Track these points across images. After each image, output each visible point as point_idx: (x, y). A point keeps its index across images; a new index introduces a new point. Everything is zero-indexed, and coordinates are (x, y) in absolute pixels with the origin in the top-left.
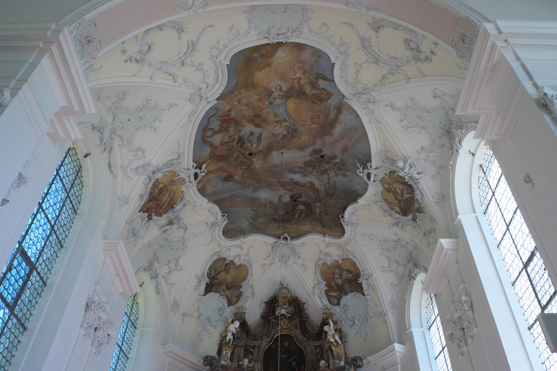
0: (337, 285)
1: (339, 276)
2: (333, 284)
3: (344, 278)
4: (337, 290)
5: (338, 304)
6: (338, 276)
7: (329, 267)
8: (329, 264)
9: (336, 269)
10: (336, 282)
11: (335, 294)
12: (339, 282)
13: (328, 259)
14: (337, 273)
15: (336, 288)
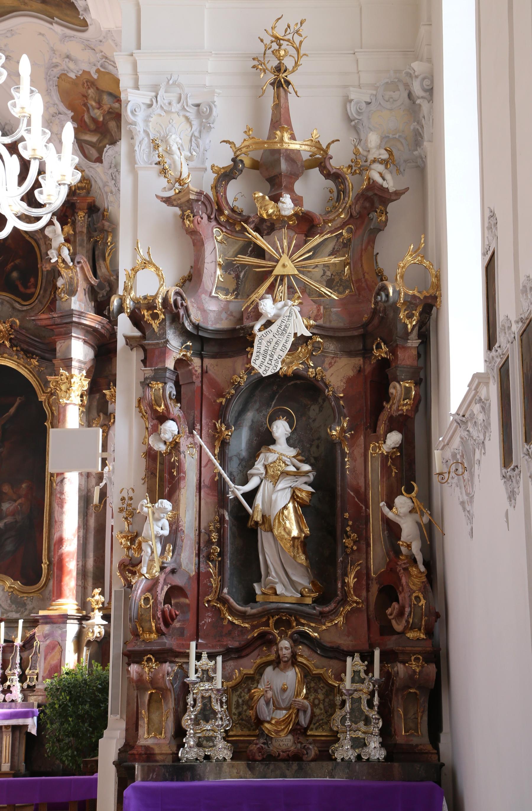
0: (94, 120)
1: (96, 102)
2: (86, 118)
3: (106, 108)
4: (95, 131)
5: (99, 160)
6: (94, 104)
7: (74, 83)
8: (74, 77)
9: (89, 88)
10: (92, 114)
11: (94, 139)
12: (98, 114)
13: (72, 65)
14: (92, 97)
15: (92, 126)
